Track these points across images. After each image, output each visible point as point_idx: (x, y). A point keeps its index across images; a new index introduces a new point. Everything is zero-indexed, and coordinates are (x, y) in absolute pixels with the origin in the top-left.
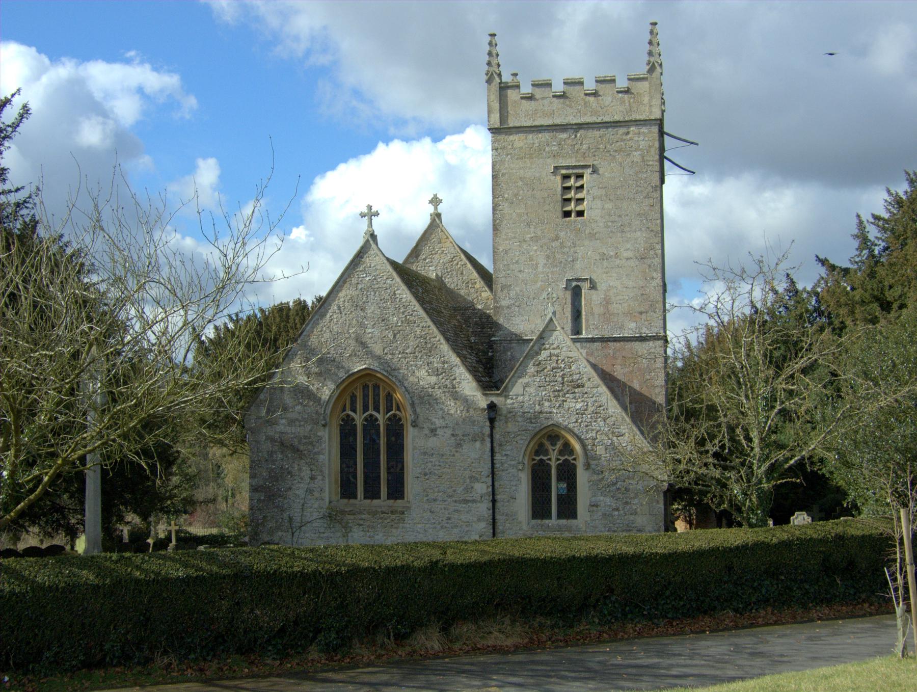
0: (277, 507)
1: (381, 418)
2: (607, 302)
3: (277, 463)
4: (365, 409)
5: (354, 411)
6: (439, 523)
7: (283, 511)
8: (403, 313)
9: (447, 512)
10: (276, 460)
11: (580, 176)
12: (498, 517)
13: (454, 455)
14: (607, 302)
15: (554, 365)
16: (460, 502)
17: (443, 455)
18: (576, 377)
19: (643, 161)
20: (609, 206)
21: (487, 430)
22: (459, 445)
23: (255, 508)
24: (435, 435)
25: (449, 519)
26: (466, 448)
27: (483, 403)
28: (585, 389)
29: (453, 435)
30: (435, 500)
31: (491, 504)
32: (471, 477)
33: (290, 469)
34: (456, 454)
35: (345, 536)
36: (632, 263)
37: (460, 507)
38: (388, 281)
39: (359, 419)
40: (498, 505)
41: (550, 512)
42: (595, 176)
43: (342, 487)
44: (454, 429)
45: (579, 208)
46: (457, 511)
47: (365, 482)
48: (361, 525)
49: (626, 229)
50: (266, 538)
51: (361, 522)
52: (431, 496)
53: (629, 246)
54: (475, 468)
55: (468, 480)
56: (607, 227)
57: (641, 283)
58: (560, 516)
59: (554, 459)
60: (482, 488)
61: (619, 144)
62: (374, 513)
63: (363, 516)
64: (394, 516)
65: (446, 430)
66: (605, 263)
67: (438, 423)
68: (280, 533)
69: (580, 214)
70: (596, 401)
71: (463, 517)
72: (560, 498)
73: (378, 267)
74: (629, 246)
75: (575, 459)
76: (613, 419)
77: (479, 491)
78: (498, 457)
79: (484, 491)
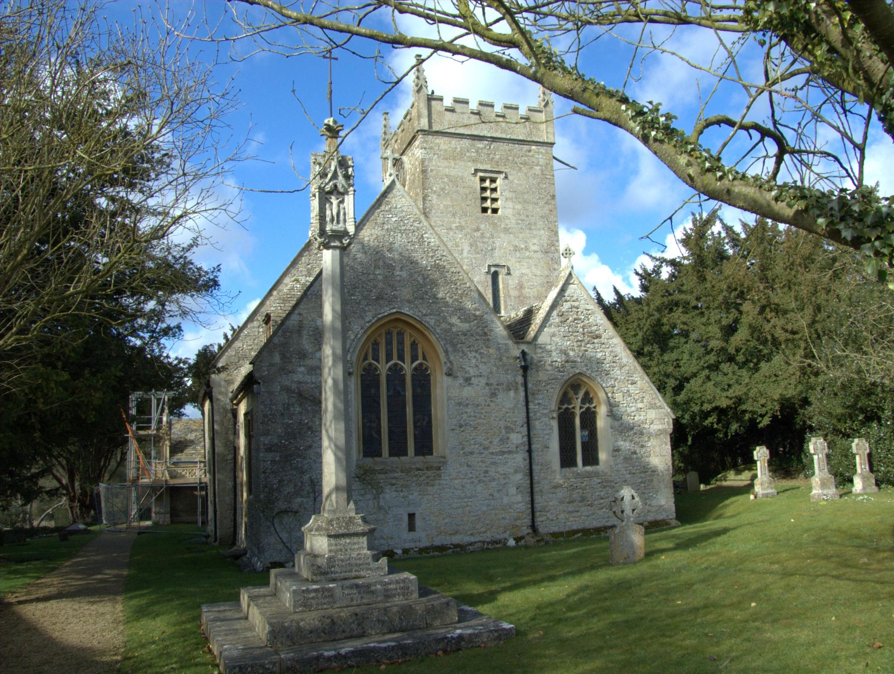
0: (296, 468)
1: (408, 368)
2: (521, 287)
3: (294, 417)
4: (389, 358)
5: (377, 360)
6: (477, 477)
7: (303, 473)
8: (432, 257)
9: (484, 465)
10: (293, 414)
11: (493, 180)
12: (534, 467)
13: (489, 405)
14: (521, 287)
15: (575, 316)
16: (496, 454)
17: (478, 405)
18: (594, 328)
19: (543, 174)
20: (519, 207)
21: (520, 379)
22: (494, 395)
23: (268, 471)
24: (470, 384)
25: (486, 472)
26: (501, 396)
27: (517, 353)
28: (602, 340)
29: (487, 384)
30: (472, 453)
31: (527, 455)
32: (507, 428)
33: (310, 424)
34: (492, 404)
35: (376, 497)
36: (539, 255)
37: (497, 458)
38: (416, 224)
39: (383, 368)
40: (534, 455)
41: (575, 460)
42: (506, 181)
43: (364, 443)
44: (488, 378)
45: (494, 206)
46: (494, 463)
47: (390, 439)
48: (393, 485)
49: (533, 227)
50: (282, 505)
51: (394, 481)
52: (467, 450)
53: (535, 241)
54: (509, 417)
55: (503, 431)
56: (518, 224)
57: (546, 273)
58: (584, 464)
59: (578, 408)
60: (517, 438)
61: (523, 158)
62: (407, 471)
63: (396, 475)
64: (429, 473)
65: (480, 379)
66: (518, 254)
67: (472, 372)
68: (299, 500)
69: (495, 211)
70: (612, 352)
71: (500, 469)
72: (584, 444)
73: (405, 209)
74: (535, 241)
75: (573, 408)
76: (627, 368)
77: (515, 442)
78: (531, 406)
79: (520, 441)
